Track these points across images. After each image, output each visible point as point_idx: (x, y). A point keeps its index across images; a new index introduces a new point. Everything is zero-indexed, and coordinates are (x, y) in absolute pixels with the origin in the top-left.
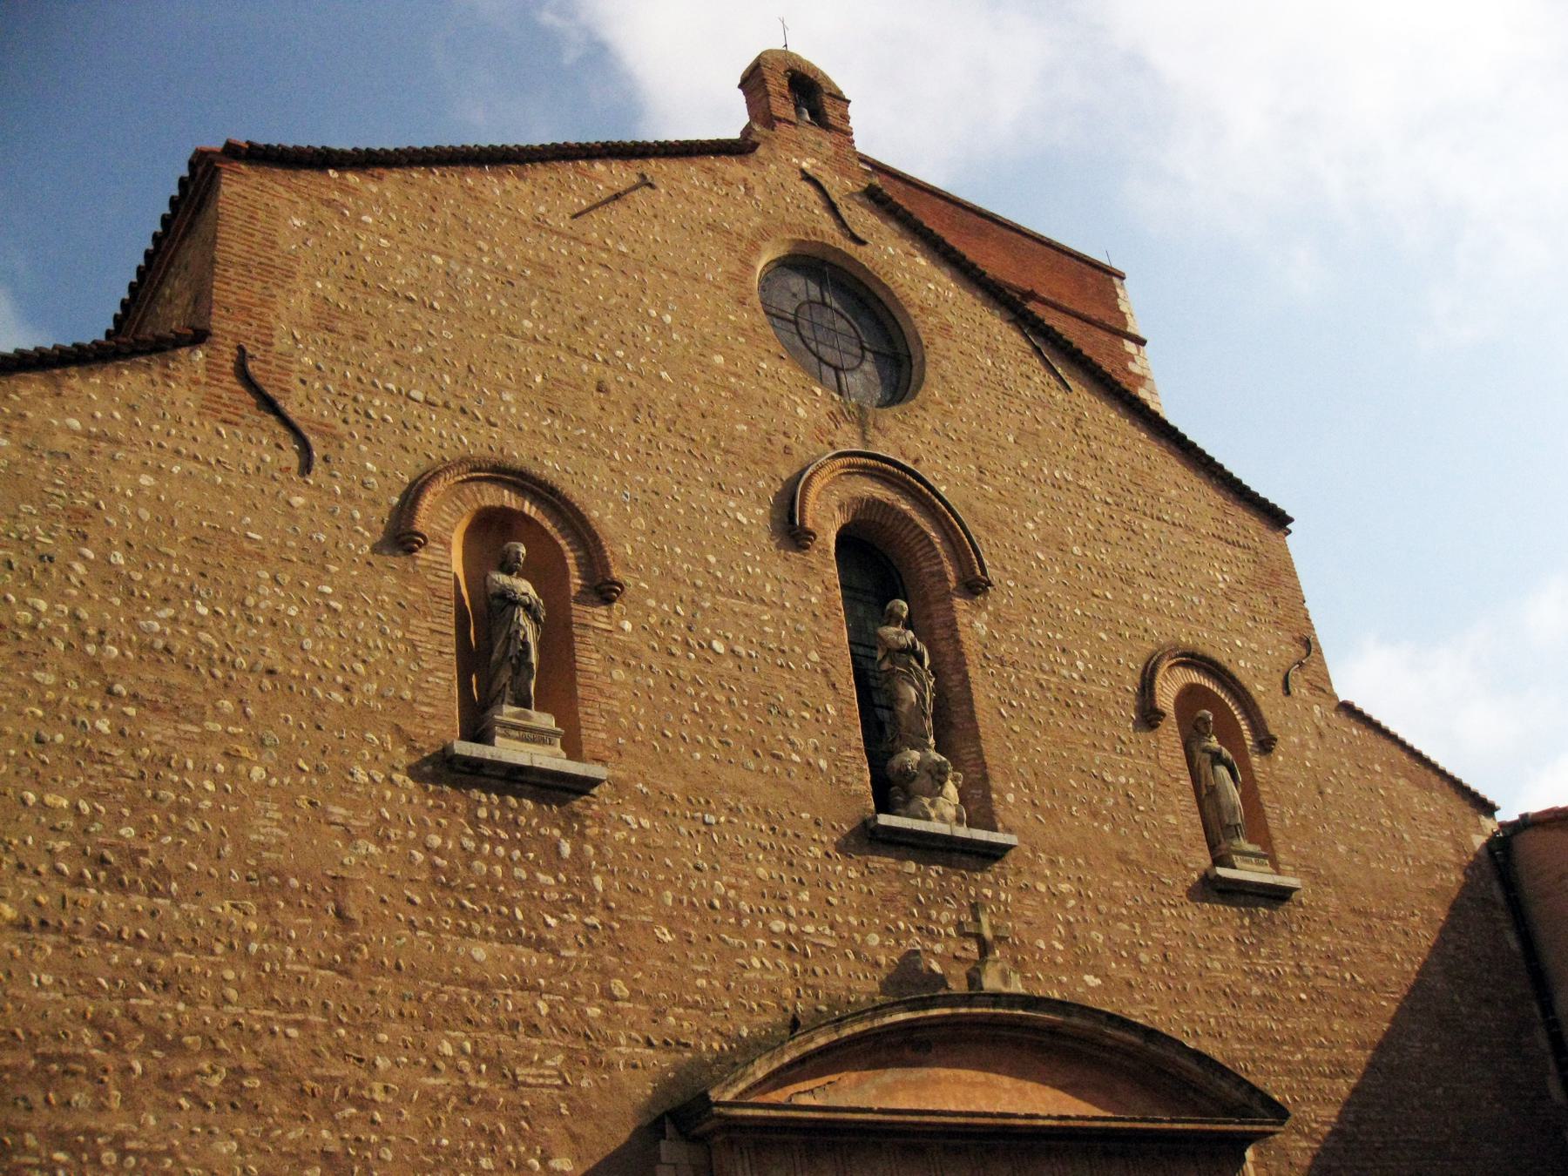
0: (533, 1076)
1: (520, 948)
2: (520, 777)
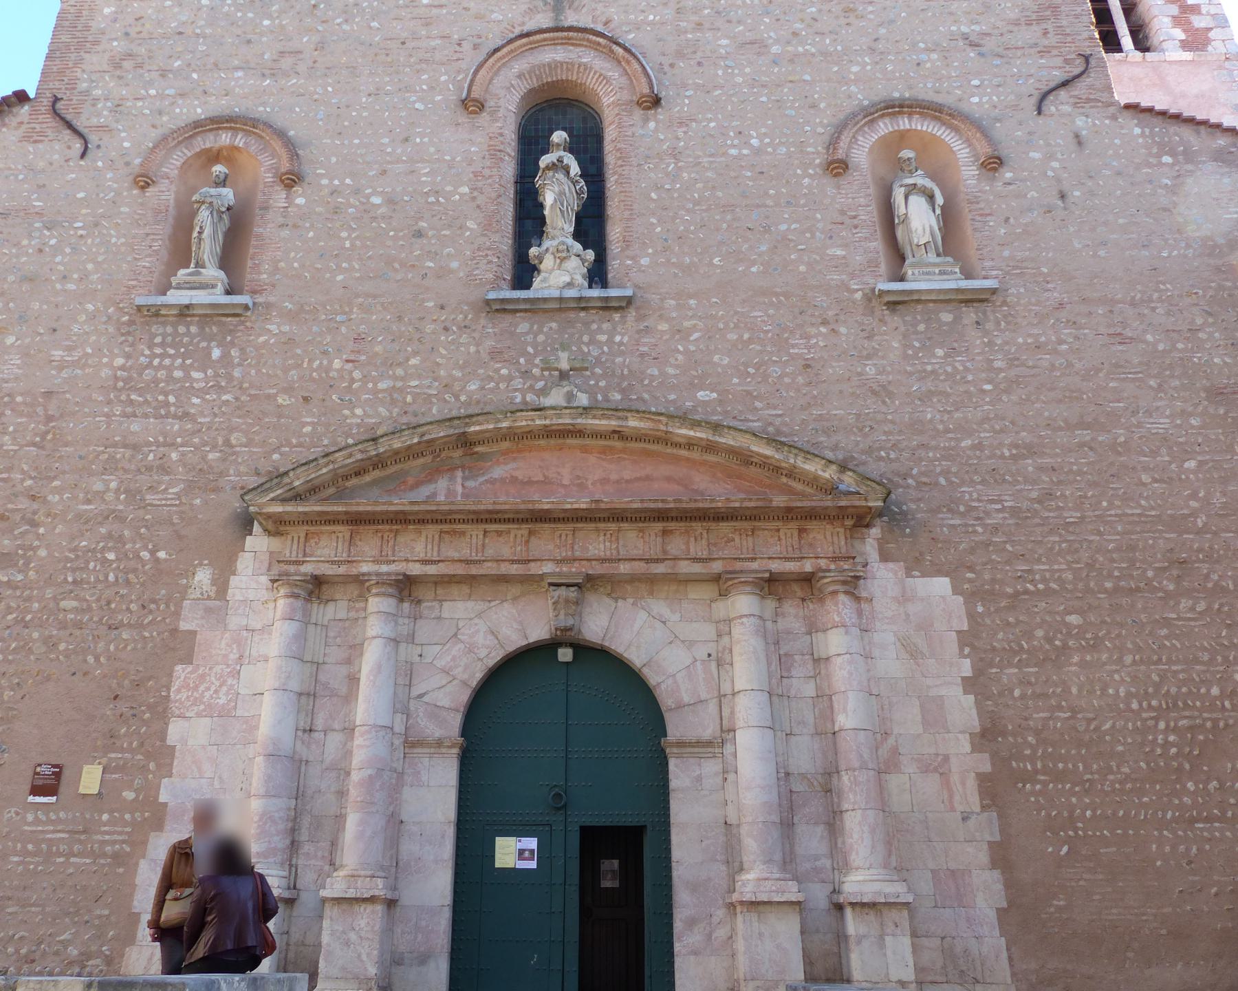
0: (158, 500)
1: (170, 420)
2: (191, 312)
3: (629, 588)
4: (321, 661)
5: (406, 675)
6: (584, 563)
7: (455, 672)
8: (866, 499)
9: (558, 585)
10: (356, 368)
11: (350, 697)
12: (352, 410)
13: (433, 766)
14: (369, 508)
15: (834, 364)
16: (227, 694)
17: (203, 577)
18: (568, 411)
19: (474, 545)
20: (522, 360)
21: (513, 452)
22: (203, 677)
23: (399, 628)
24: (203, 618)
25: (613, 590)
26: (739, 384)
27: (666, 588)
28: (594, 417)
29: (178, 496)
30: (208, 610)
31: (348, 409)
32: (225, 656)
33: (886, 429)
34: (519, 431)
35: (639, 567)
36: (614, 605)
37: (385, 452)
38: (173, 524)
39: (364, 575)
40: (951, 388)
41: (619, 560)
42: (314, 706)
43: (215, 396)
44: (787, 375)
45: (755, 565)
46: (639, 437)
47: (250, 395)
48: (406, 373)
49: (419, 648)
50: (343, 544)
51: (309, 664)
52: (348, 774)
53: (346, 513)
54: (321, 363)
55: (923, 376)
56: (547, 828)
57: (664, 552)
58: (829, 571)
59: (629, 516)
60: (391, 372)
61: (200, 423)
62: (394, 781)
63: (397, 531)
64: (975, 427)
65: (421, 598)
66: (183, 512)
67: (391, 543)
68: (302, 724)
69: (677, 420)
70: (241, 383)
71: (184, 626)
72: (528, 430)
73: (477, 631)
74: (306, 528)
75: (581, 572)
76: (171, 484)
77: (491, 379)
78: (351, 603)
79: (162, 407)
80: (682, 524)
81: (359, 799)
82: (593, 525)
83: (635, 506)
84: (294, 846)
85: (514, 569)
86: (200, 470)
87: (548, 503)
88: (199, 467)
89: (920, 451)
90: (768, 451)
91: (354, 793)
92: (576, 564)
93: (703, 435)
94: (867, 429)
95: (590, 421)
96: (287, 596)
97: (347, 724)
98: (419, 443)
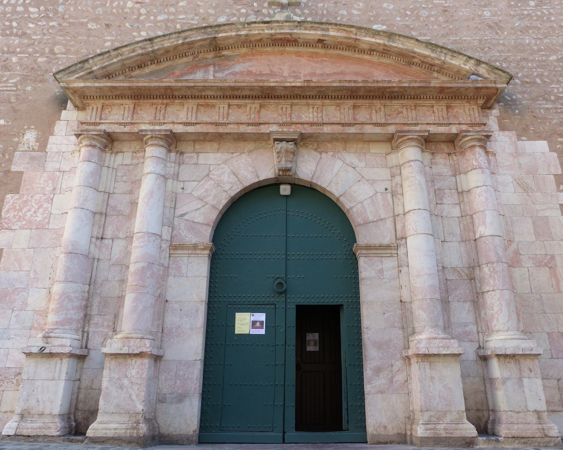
1: (13, 37)
3: (329, 145)
4: (111, 192)
5: (172, 201)
6: (299, 125)
7: (207, 199)
8: (495, 83)
9: (281, 140)
10: (142, 7)
11: (131, 216)
12: (139, 33)
13: (191, 263)
14: (146, 84)
15: (463, 10)
16: (43, 214)
17: (30, 137)
18: (287, 24)
19: (221, 114)
20: (255, 4)
21: (248, 56)
22: (26, 202)
23: (168, 169)
24: (28, 163)
25: (318, 147)
26: (401, 21)
27: (355, 146)
28: (306, 29)
29: (16, 85)
30: (33, 158)
31: (136, 32)
32: (43, 188)
33: (499, 49)
34: (253, 39)
35: (338, 129)
36: (319, 156)
37: (159, 49)
38: (11, 103)
39: (142, 131)
40: (541, 25)
41: (324, 124)
42: (105, 222)
43: (45, 23)
44: (432, 16)
45: (418, 128)
46: (337, 45)
47: (69, 23)
48: (177, 11)
49: (181, 185)
50: (128, 112)
51: (102, 194)
52: (128, 267)
53: (130, 88)
54: (119, 4)
55: (522, 17)
56: (273, 307)
57: (355, 119)
58: (469, 131)
59: (330, 94)
60: (166, 10)
61: (33, 39)
62: (161, 273)
63: (167, 105)
64: (558, 48)
65: (183, 150)
66: (18, 95)
67: (163, 112)
68: (95, 234)
69: (363, 31)
70: (64, 15)
71: (14, 168)
72: (258, 38)
73: (224, 172)
74: (102, 101)
75: (297, 132)
76: (11, 77)
77: (234, 15)
78: (134, 154)
79: (8, 29)
80: (367, 101)
81: (134, 283)
82: (305, 101)
83: (335, 85)
84: (87, 318)
85: (250, 129)
86: (32, 68)
87: (274, 82)
88: (31, 67)
89: (522, 63)
90: (427, 52)
91: (131, 280)
92: (293, 126)
93: (381, 42)
94: (487, 49)
95: (303, 32)
96: (87, 146)
97: (128, 234)
98: (183, 44)
